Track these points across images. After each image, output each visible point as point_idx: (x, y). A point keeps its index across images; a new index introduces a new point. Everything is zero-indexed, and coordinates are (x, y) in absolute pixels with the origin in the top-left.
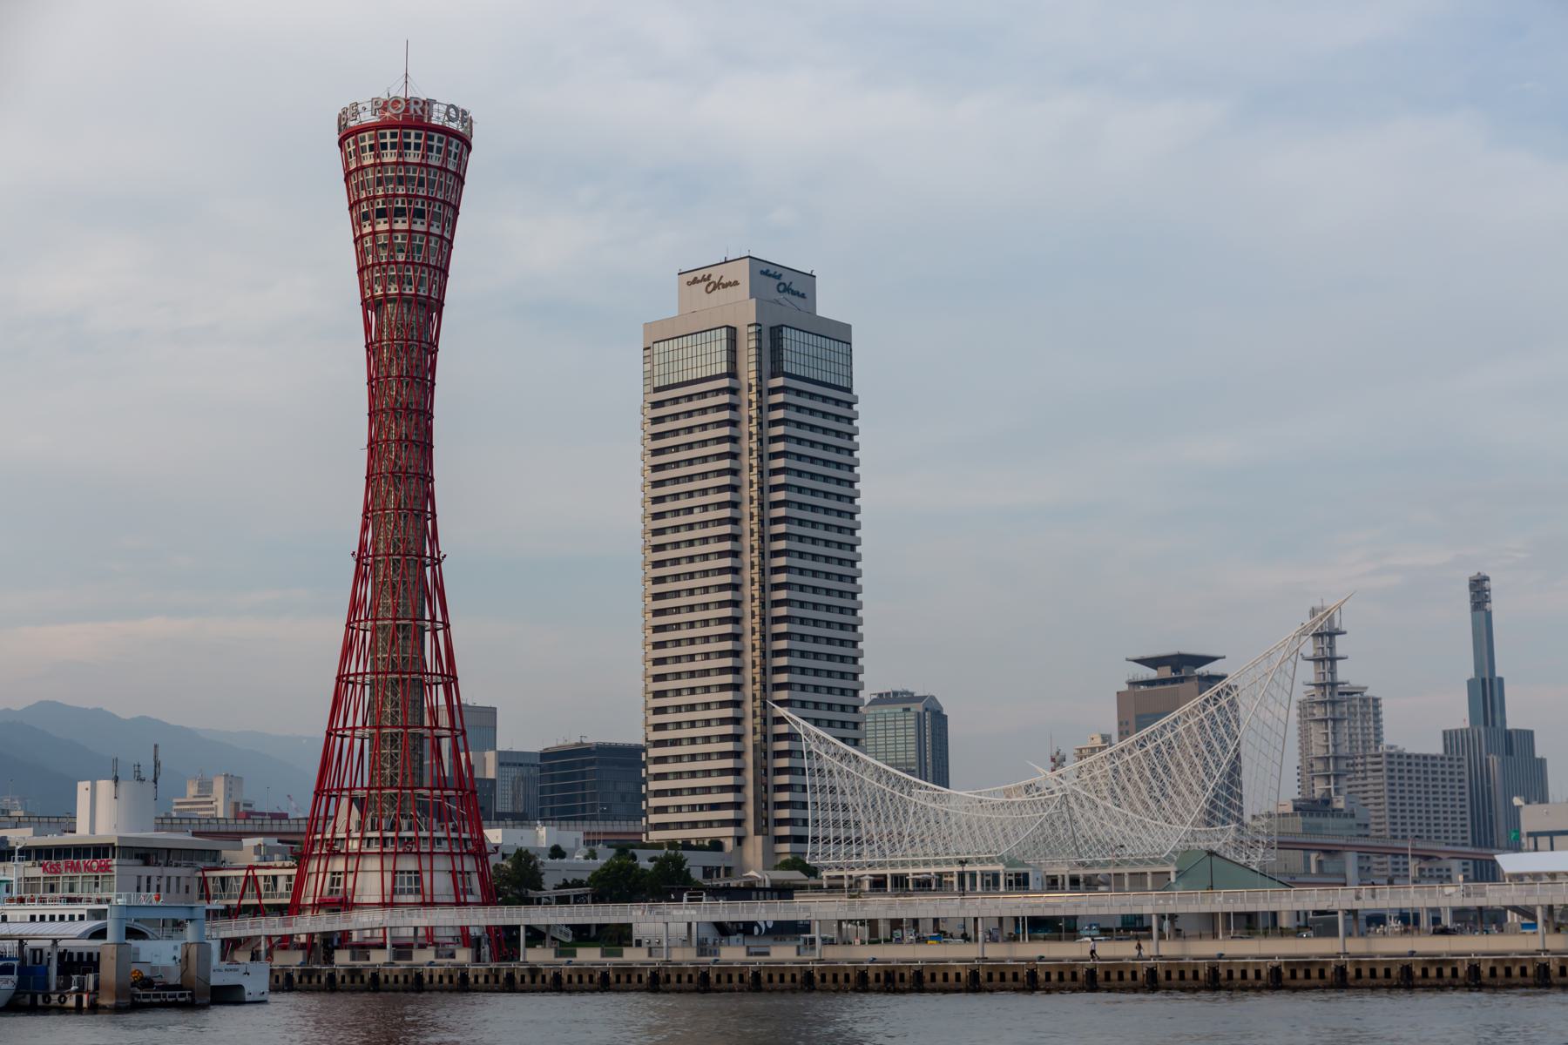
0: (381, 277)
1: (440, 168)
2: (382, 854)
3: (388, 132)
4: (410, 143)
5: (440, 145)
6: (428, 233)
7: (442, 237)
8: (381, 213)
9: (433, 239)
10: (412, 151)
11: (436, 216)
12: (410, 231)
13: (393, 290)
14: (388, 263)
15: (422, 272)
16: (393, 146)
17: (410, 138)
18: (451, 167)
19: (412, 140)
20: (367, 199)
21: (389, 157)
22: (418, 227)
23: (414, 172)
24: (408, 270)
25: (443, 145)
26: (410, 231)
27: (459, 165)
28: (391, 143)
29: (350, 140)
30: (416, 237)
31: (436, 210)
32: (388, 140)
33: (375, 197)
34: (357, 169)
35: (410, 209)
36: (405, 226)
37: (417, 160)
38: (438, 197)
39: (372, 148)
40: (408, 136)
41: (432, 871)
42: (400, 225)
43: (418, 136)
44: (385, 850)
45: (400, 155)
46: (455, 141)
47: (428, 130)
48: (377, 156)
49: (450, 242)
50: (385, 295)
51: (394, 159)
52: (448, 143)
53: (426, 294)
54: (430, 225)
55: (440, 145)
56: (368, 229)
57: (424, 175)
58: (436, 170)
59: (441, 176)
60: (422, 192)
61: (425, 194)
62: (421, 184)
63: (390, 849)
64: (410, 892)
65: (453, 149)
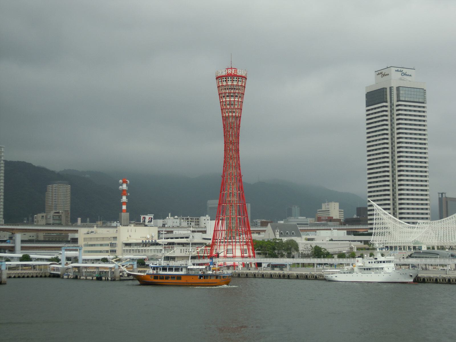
0: (228, 111)
1: (241, 85)
2: (224, 245)
3: (224, 78)
5: (236, 79)
6: (238, 101)
7: (241, 101)
8: (224, 96)
9: (239, 102)
10: (230, 82)
11: (236, 96)
13: (230, 114)
14: (226, 108)
15: (237, 110)
16: (226, 81)
17: (234, 79)
18: (243, 85)
19: (230, 79)
20: (221, 93)
22: (236, 99)
23: (235, 87)
25: (241, 80)
26: (234, 101)
27: (242, 83)
28: (230, 80)
31: (236, 95)
32: (230, 79)
33: (222, 93)
36: (233, 99)
37: (236, 84)
38: (237, 92)
41: (235, 249)
42: (232, 99)
43: (236, 78)
44: (236, 244)
45: (232, 83)
46: (244, 79)
48: (222, 83)
49: (242, 102)
50: (229, 116)
51: (231, 84)
52: (243, 79)
53: (232, 115)
54: (239, 99)
55: (236, 79)
56: (221, 101)
60: (232, 91)
62: (237, 89)
63: (234, 244)
64: (231, 253)
65: (240, 80)
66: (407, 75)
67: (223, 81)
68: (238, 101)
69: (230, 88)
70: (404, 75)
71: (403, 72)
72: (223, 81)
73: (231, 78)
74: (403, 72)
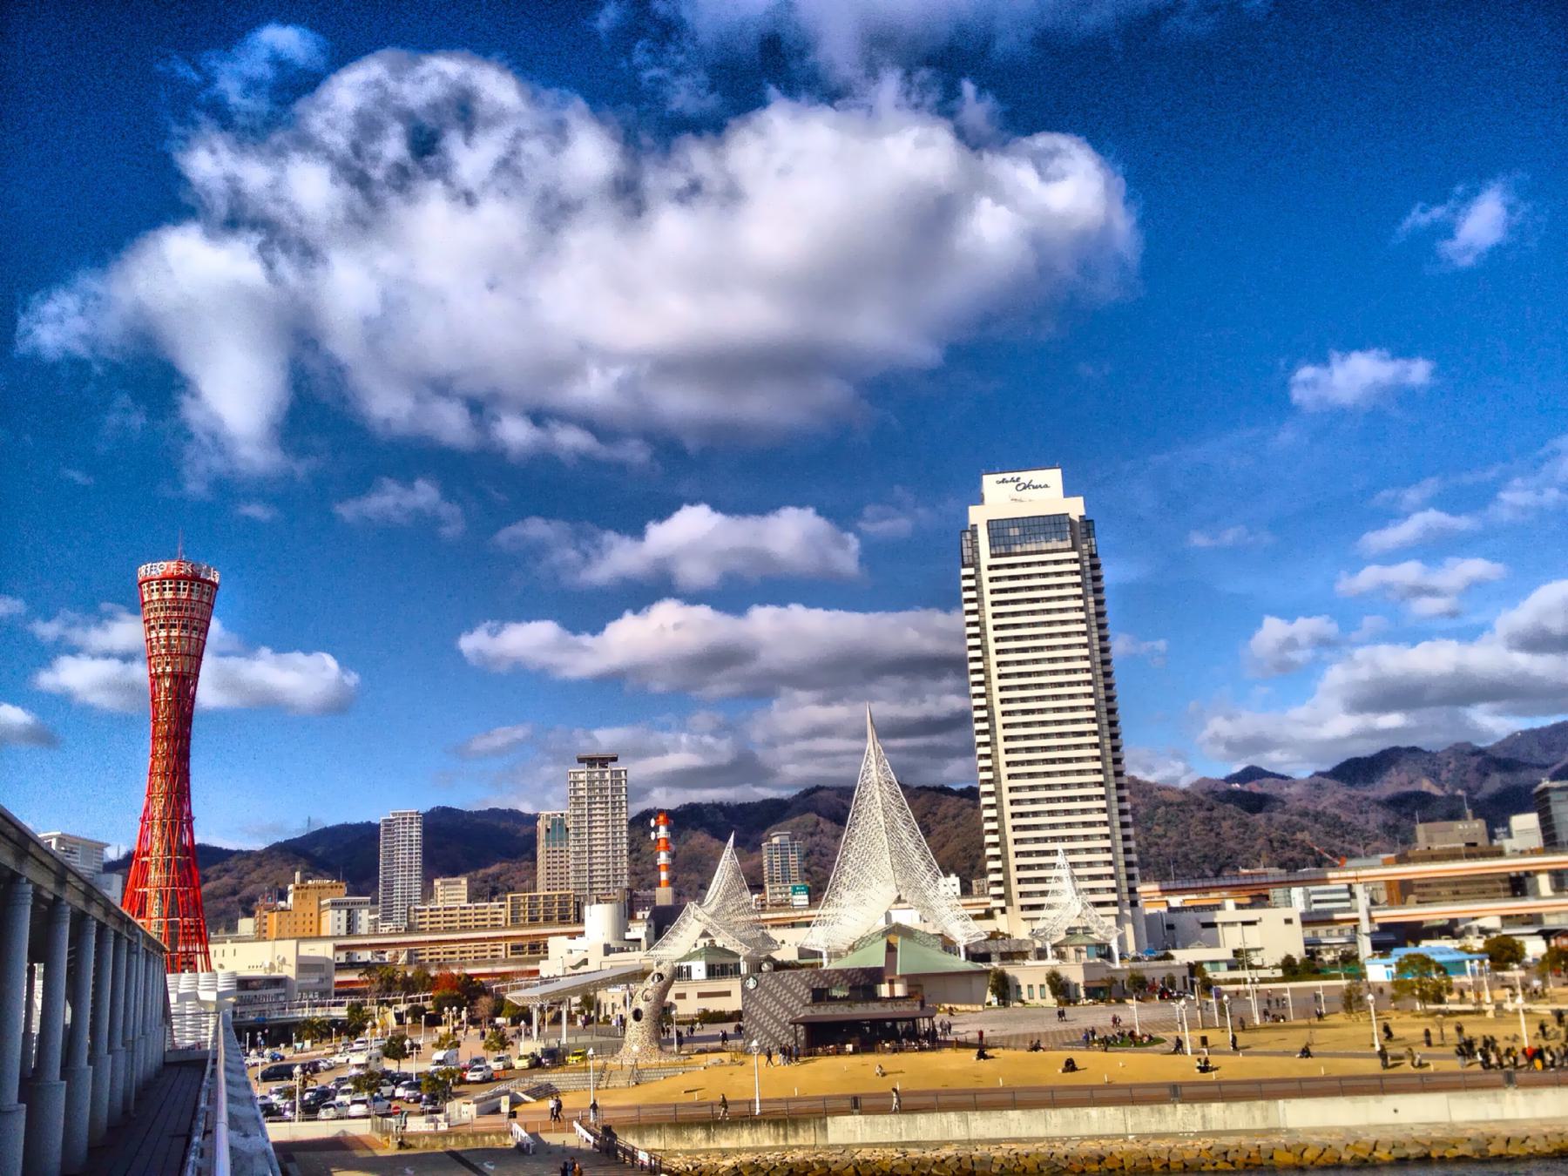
6: (190, 637)
8: (162, 626)
21: (168, 595)
29: (145, 584)
34: (149, 602)
39: (157, 590)
40: (179, 584)
42: (174, 633)
46: (208, 586)
49: (204, 642)
51: (171, 596)
62: (186, 610)
66: (1034, 487)
67: (153, 591)
68: (198, 639)
69: (167, 608)
70: (1025, 488)
71: (1021, 481)
72: (153, 591)
73: (170, 583)
74: (1021, 481)
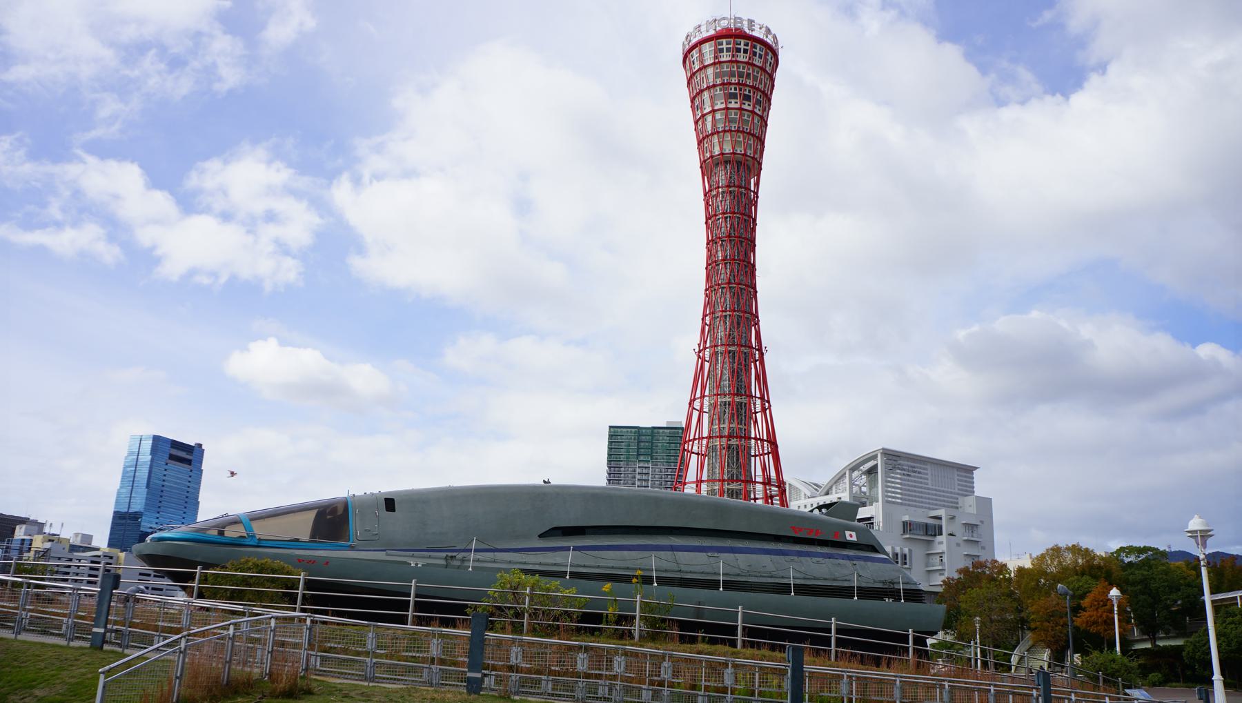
4: (740, 49)
6: (753, 112)
12: (741, 109)
18: (768, 69)
24: (739, 137)
25: (763, 53)
26: (741, 109)
30: (745, 114)
35: (740, 94)
47: (754, 41)
52: (766, 54)
57: (751, 71)
58: (758, 70)
59: (761, 75)
61: (751, 84)
